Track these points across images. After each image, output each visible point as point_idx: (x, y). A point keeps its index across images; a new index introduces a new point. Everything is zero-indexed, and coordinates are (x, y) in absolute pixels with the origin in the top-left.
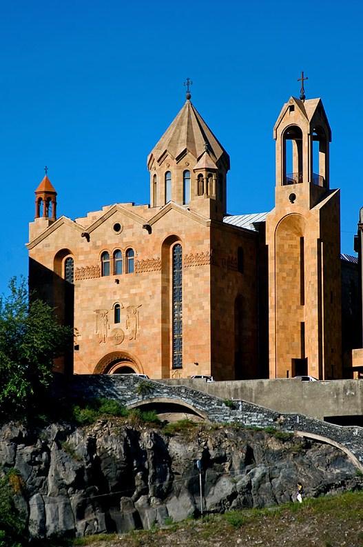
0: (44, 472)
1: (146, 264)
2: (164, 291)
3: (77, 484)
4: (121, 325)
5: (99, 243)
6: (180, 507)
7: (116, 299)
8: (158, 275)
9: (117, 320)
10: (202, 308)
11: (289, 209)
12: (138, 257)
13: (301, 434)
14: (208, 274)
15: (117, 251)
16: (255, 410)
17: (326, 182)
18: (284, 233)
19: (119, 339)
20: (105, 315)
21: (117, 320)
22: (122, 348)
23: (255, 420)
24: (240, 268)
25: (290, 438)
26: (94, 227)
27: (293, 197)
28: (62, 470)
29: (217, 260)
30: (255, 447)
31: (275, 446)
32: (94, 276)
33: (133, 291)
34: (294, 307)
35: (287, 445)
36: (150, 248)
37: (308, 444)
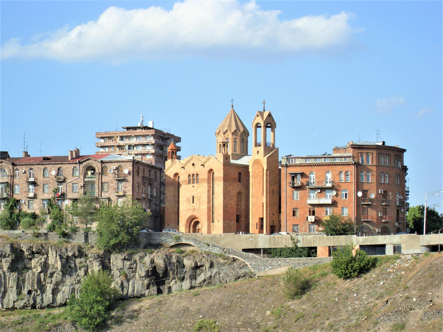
0: (135, 272)
1: (203, 180)
2: (209, 191)
3: (147, 275)
4: (194, 204)
5: (188, 171)
6: (186, 284)
7: (193, 194)
8: (206, 185)
9: (193, 202)
10: (220, 199)
11: (257, 157)
12: (200, 177)
13: (232, 256)
14: (222, 185)
15: (193, 174)
16: (216, 247)
17: (274, 145)
18: (256, 167)
19: (194, 210)
20: (189, 200)
21: (193, 202)
22: (195, 214)
23: (216, 251)
24: (240, 181)
25: (228, 258)
26: (186, 164)
27: (258, 152)
28: (141, 271)
29: (226, 179)
30: (214, 261)
31: (222, 261)
32: (186, 184)
33: (198, 191)
34: (260, 197)
35: (226, 261)
36: (204, 175)
37: (234, 260)
